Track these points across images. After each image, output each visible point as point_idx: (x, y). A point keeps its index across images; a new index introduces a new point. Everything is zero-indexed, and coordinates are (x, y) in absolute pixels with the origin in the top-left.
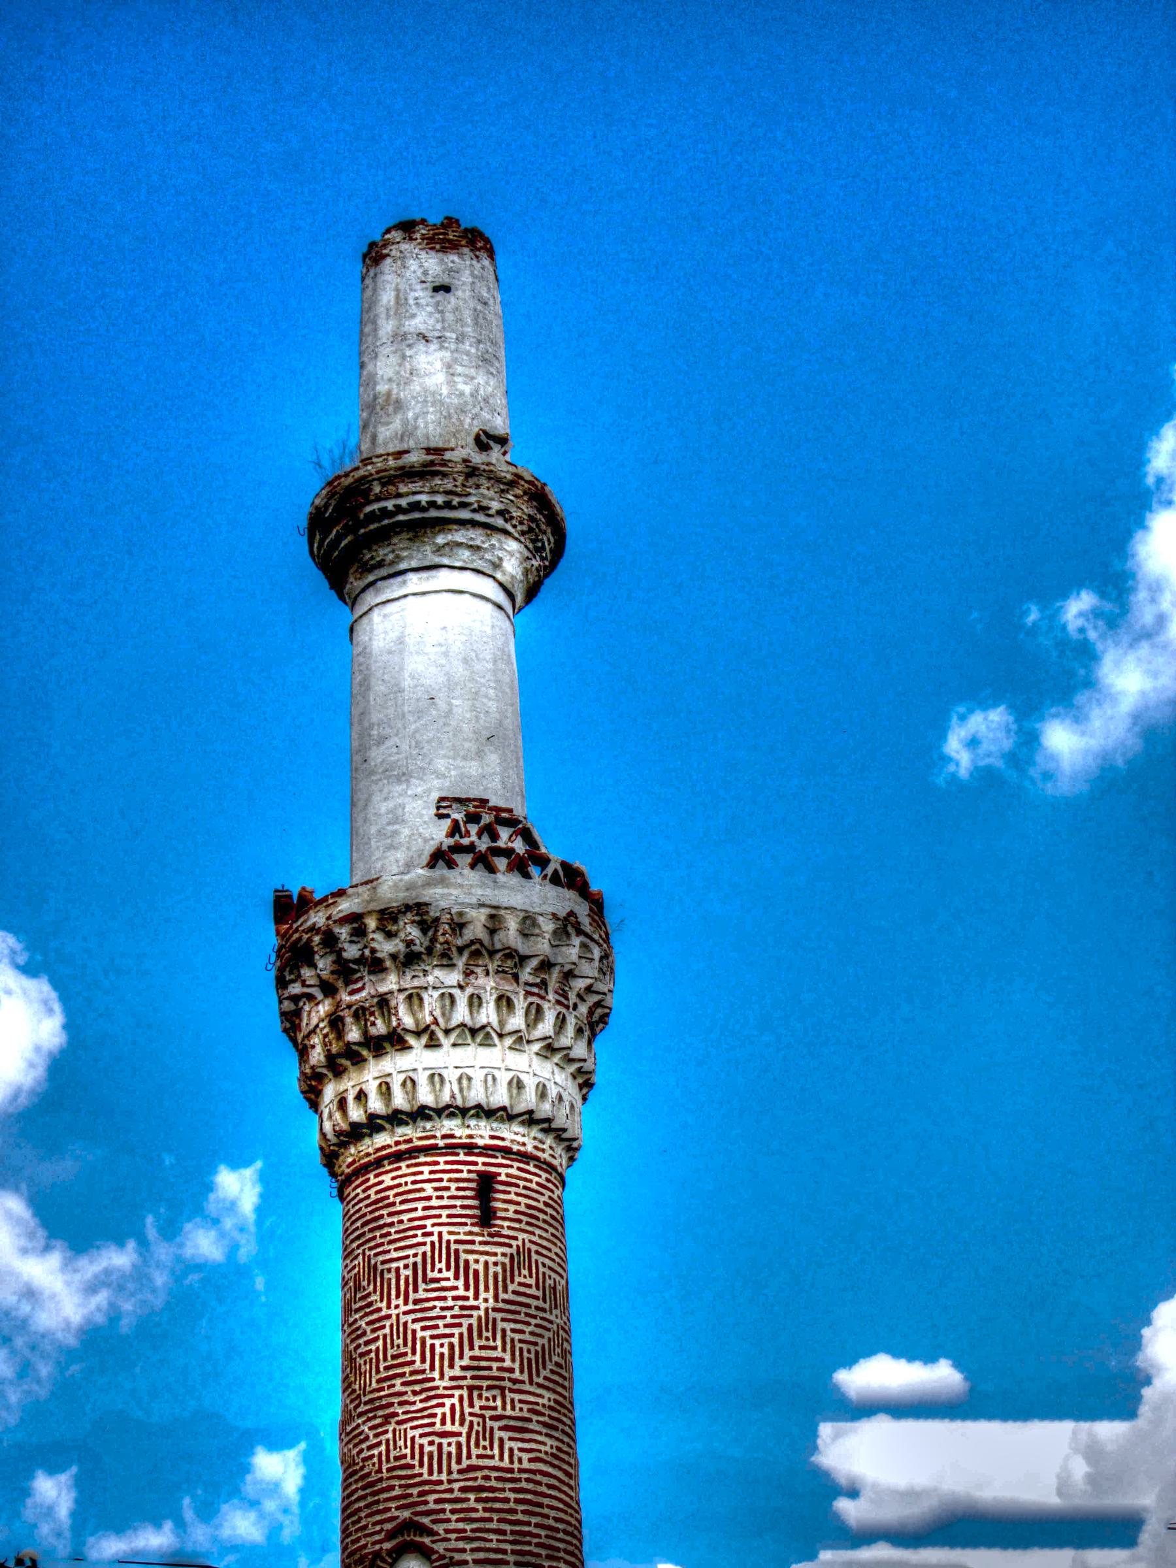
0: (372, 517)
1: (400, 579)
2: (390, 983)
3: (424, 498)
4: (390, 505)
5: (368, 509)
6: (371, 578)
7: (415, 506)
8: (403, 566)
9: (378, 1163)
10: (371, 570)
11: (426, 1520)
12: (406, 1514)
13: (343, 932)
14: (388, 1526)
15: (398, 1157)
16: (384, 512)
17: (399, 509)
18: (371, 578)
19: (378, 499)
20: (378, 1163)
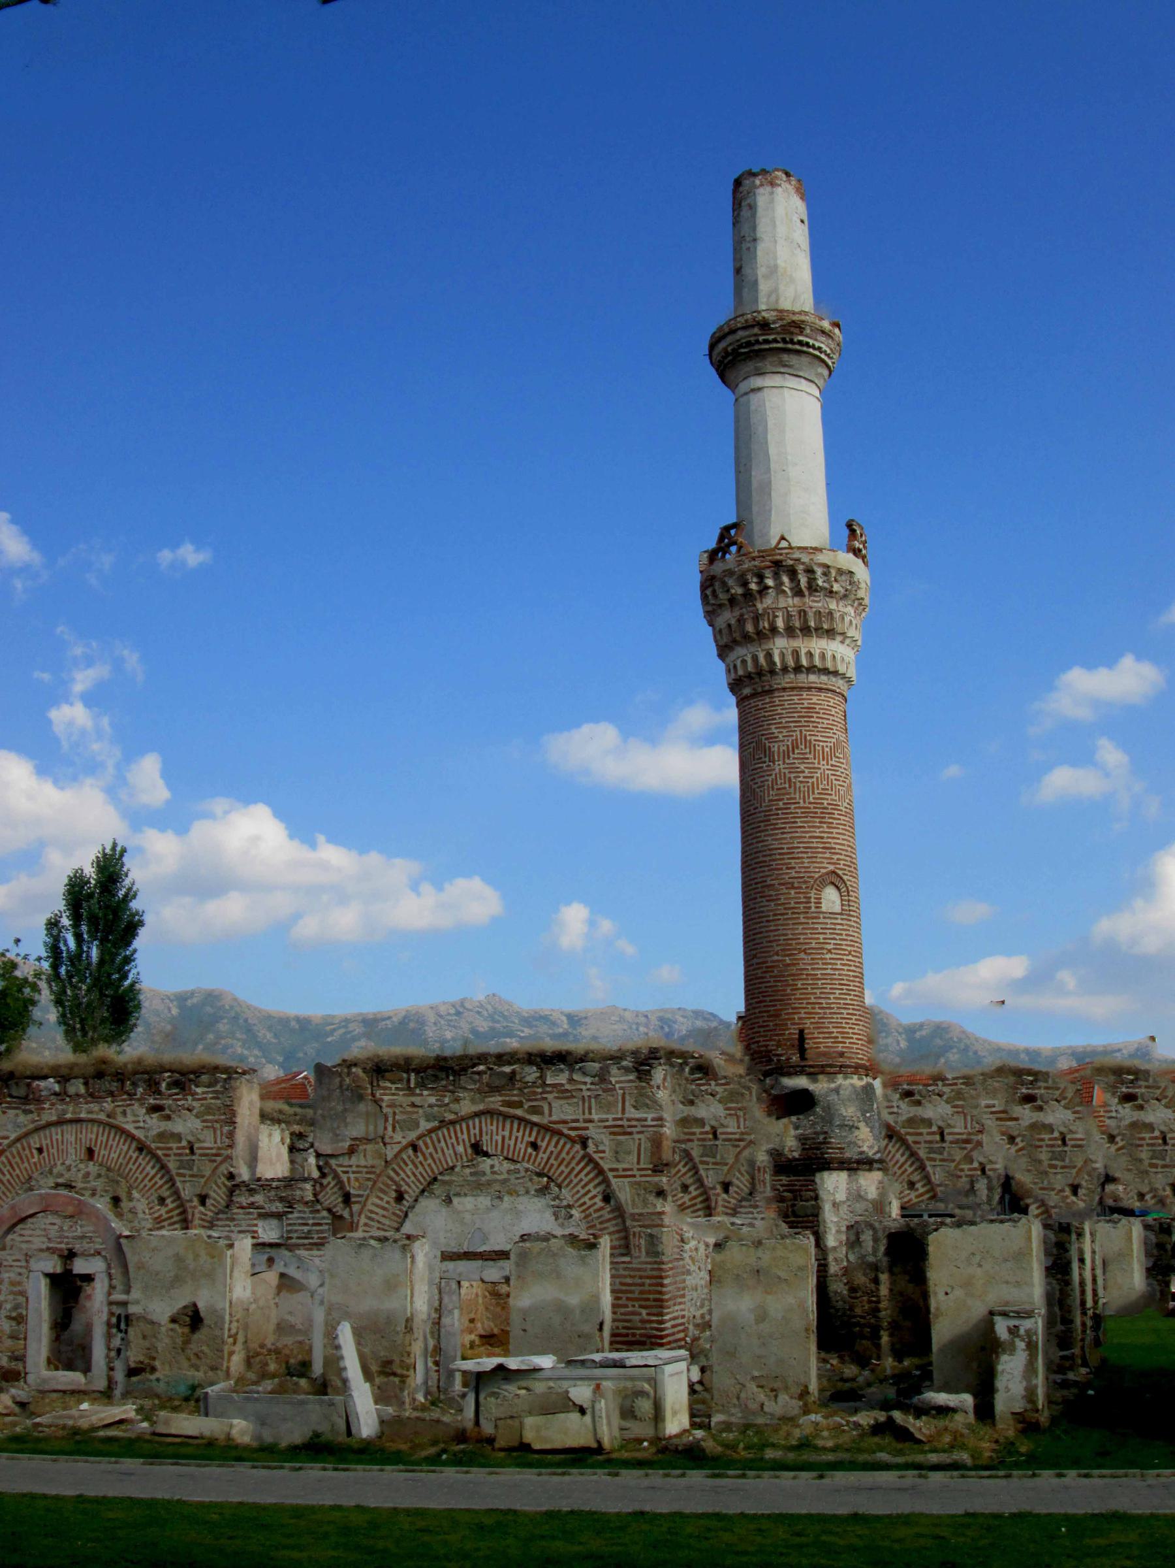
0: (800, 343)
1: (798, 379)
2: (833, 605)
3: (824, 347)
4: (811, 342)
5: (801, 338)
6: (782, 370)
7: (819, 349)
8: (801, 374)
9: (809, 689)
10: (785, 366)
11: (840, 872)
12: (831, 867)
13: (819, 571)
14: (823, 871)
15: (820, 689)
16: (807, 345)
17: (813, 347)
18: (782, 370)
19: (807, 336)
20: (809, 689)
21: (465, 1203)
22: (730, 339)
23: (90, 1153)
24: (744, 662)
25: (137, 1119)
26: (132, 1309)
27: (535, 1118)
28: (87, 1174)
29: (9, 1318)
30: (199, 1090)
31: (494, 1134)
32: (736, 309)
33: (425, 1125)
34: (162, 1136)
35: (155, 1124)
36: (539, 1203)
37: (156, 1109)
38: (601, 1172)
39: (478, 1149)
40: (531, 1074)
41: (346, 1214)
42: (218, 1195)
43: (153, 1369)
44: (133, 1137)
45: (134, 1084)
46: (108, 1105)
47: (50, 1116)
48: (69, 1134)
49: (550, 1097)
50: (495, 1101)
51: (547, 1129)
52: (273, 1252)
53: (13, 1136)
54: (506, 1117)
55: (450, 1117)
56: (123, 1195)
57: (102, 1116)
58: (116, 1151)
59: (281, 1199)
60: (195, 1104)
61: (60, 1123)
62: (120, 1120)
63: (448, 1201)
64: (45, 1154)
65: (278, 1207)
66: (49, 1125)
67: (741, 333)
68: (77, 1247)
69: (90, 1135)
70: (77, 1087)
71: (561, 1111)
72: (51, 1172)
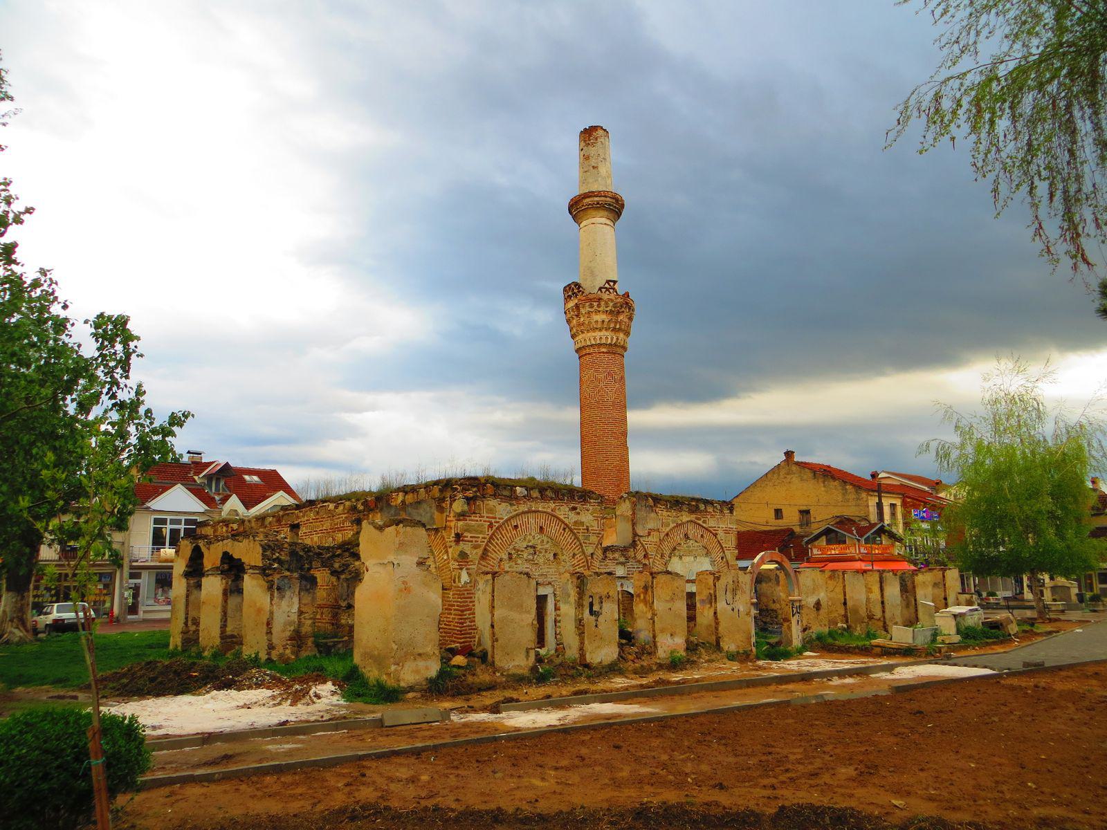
21: (686, 559)
22: (603, 198)
23: (541, 528)
24: (607, 338)
25: (563, 511)
26: (803, 603)
27: (704, 525)
28: (543, 541)
30: (592, 501)
31: (692, 531)
32: (584, 181)
33: (672, 525)
34: (576, 523)
35: (572, 515)
36: (707, 560)
37: (574, 509)
38: (722, 548)
39: (687, 537)
40: (702, 507)
41: (647, 563)
42: (599, 553)
43: (810, 628)
44: (563, 522)
45: (563, 495)
46: (552, 505)
47: (523, 508)
48: (532, 519)
49: (709, 517)
50: (693, 517)
51: (707, 529)
52: (623, 581)
54: (695, 523)
55: (680, 522)
56: (560, 553)
57: (549, 510)
58: (554, 529)
59: (624, 556)
60: (591, 508)
61: (529, 512)
62: (557, 513)
63: (681, 557)
64: (520, 529)
65: (622, 559)
66: (524, 513)
67: (608, 199)
68: (540, 581)
69: (542, 520)
70: (535, 494)
71: (711, 523)
72: (525, 539)
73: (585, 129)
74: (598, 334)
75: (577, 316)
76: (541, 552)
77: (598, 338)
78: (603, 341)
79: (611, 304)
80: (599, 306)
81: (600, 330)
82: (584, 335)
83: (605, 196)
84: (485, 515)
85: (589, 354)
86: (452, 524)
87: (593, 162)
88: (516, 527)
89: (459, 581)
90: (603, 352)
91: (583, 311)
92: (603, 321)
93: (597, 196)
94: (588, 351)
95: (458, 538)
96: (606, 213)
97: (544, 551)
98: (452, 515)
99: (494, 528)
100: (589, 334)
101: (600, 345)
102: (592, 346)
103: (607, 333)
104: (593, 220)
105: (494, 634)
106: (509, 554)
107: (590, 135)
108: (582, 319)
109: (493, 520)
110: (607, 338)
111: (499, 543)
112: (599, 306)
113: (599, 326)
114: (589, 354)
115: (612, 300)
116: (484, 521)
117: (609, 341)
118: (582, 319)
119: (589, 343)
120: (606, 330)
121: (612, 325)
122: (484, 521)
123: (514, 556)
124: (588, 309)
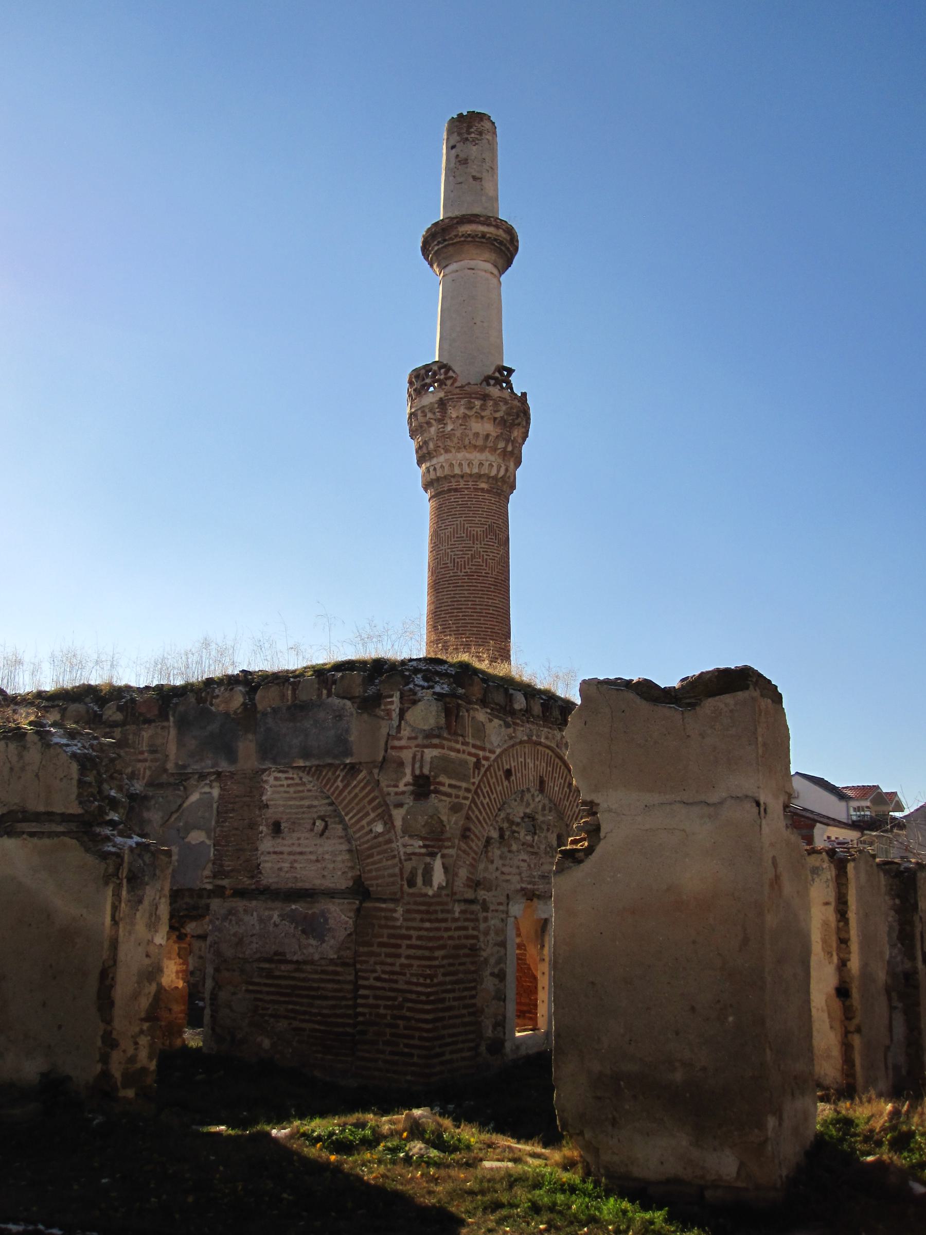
22: (492, 230)
24: (491, 465)
29: (492, 974)
53: (498, 751)
64: (513, 778)
73: (460, 116)
74: (476, 456)
75: (440, 421)
76: (541, 829)
77: (476, 463)
78: (484, 470)
79: (504, 408)
80: (483, 407)
81: (482, 449)
82: (449, 456)
83: (497, 227)
84: (470, 740)
85: (456, 490)
86: (407, 755)
87: (473, 169)
88: (508, 773)
89: (428, 881)
90: (482, 490)
91: (453, 413)
92: (487, 436)
93: (483, 224)
94: (454, 485)
95: (423, 787)
96: (493, 256)
97: (545, 827)
98: (406, 732)
99: (483, 770)
100: (459, 456)
101: (479, 476)
102: (445, 477)
103: (492, 458)
104: (472, 263)
105: (848, 1013)
106: (501, 830)
107: (470, 127)
108: (449, 427)
109: (481, 753)
110: (491, 465)
111: (485, 802)
112: (483, 407)
113: (480, 442)
114: (456, 490)
115: (505, 402)
116: (470, 754)
117: (493, 473)
118: (449, 427)
119: (457, 471)
120: (494, 450)
121: (501, 445)
122: (470, 754)
123: (507, 833)
124: (462, 410)
